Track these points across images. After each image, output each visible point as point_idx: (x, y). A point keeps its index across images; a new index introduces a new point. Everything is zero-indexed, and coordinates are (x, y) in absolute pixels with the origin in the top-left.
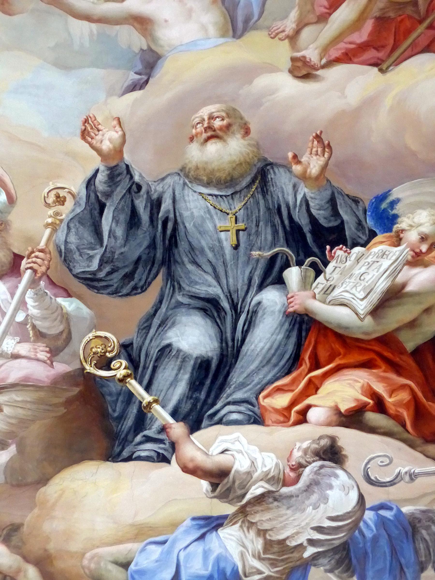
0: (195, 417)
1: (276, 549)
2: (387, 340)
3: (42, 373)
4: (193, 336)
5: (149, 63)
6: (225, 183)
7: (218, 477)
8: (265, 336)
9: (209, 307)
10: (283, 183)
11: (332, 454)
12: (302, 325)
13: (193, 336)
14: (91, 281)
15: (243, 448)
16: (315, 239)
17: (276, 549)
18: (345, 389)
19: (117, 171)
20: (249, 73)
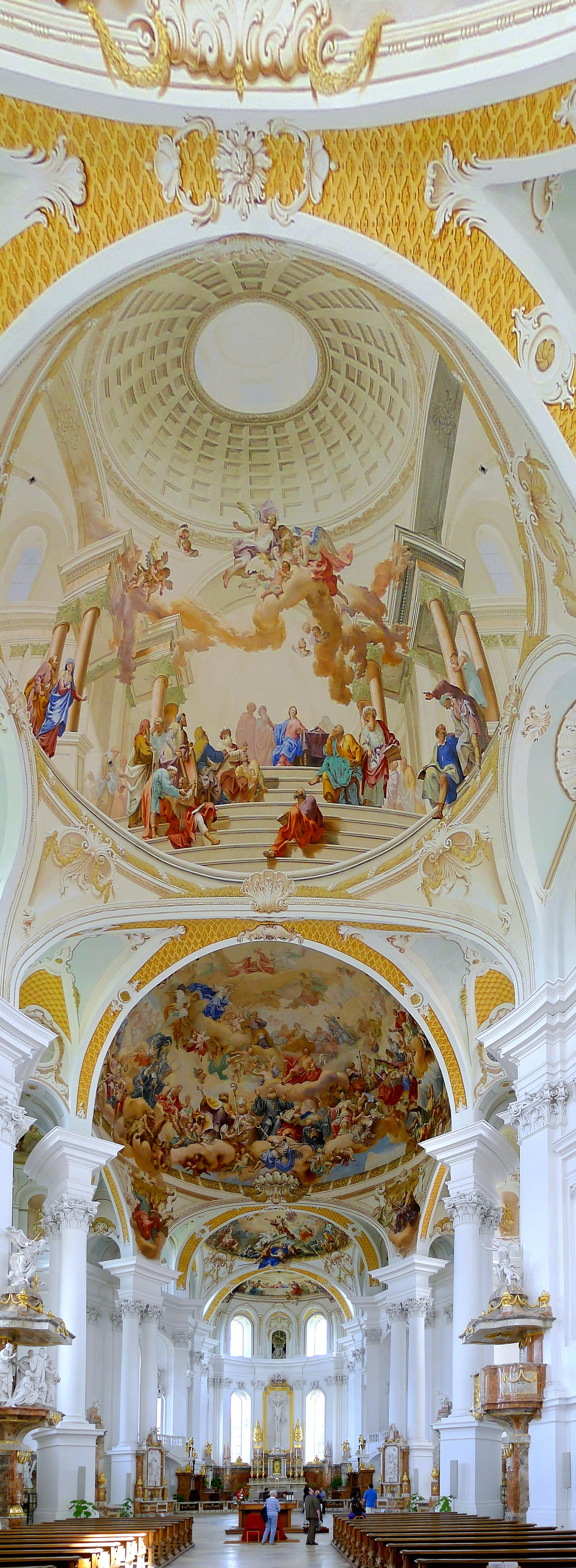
0: (269, 1134)
1: (279, 1154)
2: (292, 1124)
3: (251, 1128)
4: (269, 1122)
5: (263, 1081)
7: (272, 1143)
8: (277, 1122)
9: (271, 1118)
10: (280, 1100)
11: (285, 1140)
12: (282, 1121)
13: (269, 1122)
14: (256, 1114)
15: (275, 1139)
16: (284, 1108)
17: (279, 1154)
18: (287, 1131)
19: (259, 1098)
20: (276, 1084)
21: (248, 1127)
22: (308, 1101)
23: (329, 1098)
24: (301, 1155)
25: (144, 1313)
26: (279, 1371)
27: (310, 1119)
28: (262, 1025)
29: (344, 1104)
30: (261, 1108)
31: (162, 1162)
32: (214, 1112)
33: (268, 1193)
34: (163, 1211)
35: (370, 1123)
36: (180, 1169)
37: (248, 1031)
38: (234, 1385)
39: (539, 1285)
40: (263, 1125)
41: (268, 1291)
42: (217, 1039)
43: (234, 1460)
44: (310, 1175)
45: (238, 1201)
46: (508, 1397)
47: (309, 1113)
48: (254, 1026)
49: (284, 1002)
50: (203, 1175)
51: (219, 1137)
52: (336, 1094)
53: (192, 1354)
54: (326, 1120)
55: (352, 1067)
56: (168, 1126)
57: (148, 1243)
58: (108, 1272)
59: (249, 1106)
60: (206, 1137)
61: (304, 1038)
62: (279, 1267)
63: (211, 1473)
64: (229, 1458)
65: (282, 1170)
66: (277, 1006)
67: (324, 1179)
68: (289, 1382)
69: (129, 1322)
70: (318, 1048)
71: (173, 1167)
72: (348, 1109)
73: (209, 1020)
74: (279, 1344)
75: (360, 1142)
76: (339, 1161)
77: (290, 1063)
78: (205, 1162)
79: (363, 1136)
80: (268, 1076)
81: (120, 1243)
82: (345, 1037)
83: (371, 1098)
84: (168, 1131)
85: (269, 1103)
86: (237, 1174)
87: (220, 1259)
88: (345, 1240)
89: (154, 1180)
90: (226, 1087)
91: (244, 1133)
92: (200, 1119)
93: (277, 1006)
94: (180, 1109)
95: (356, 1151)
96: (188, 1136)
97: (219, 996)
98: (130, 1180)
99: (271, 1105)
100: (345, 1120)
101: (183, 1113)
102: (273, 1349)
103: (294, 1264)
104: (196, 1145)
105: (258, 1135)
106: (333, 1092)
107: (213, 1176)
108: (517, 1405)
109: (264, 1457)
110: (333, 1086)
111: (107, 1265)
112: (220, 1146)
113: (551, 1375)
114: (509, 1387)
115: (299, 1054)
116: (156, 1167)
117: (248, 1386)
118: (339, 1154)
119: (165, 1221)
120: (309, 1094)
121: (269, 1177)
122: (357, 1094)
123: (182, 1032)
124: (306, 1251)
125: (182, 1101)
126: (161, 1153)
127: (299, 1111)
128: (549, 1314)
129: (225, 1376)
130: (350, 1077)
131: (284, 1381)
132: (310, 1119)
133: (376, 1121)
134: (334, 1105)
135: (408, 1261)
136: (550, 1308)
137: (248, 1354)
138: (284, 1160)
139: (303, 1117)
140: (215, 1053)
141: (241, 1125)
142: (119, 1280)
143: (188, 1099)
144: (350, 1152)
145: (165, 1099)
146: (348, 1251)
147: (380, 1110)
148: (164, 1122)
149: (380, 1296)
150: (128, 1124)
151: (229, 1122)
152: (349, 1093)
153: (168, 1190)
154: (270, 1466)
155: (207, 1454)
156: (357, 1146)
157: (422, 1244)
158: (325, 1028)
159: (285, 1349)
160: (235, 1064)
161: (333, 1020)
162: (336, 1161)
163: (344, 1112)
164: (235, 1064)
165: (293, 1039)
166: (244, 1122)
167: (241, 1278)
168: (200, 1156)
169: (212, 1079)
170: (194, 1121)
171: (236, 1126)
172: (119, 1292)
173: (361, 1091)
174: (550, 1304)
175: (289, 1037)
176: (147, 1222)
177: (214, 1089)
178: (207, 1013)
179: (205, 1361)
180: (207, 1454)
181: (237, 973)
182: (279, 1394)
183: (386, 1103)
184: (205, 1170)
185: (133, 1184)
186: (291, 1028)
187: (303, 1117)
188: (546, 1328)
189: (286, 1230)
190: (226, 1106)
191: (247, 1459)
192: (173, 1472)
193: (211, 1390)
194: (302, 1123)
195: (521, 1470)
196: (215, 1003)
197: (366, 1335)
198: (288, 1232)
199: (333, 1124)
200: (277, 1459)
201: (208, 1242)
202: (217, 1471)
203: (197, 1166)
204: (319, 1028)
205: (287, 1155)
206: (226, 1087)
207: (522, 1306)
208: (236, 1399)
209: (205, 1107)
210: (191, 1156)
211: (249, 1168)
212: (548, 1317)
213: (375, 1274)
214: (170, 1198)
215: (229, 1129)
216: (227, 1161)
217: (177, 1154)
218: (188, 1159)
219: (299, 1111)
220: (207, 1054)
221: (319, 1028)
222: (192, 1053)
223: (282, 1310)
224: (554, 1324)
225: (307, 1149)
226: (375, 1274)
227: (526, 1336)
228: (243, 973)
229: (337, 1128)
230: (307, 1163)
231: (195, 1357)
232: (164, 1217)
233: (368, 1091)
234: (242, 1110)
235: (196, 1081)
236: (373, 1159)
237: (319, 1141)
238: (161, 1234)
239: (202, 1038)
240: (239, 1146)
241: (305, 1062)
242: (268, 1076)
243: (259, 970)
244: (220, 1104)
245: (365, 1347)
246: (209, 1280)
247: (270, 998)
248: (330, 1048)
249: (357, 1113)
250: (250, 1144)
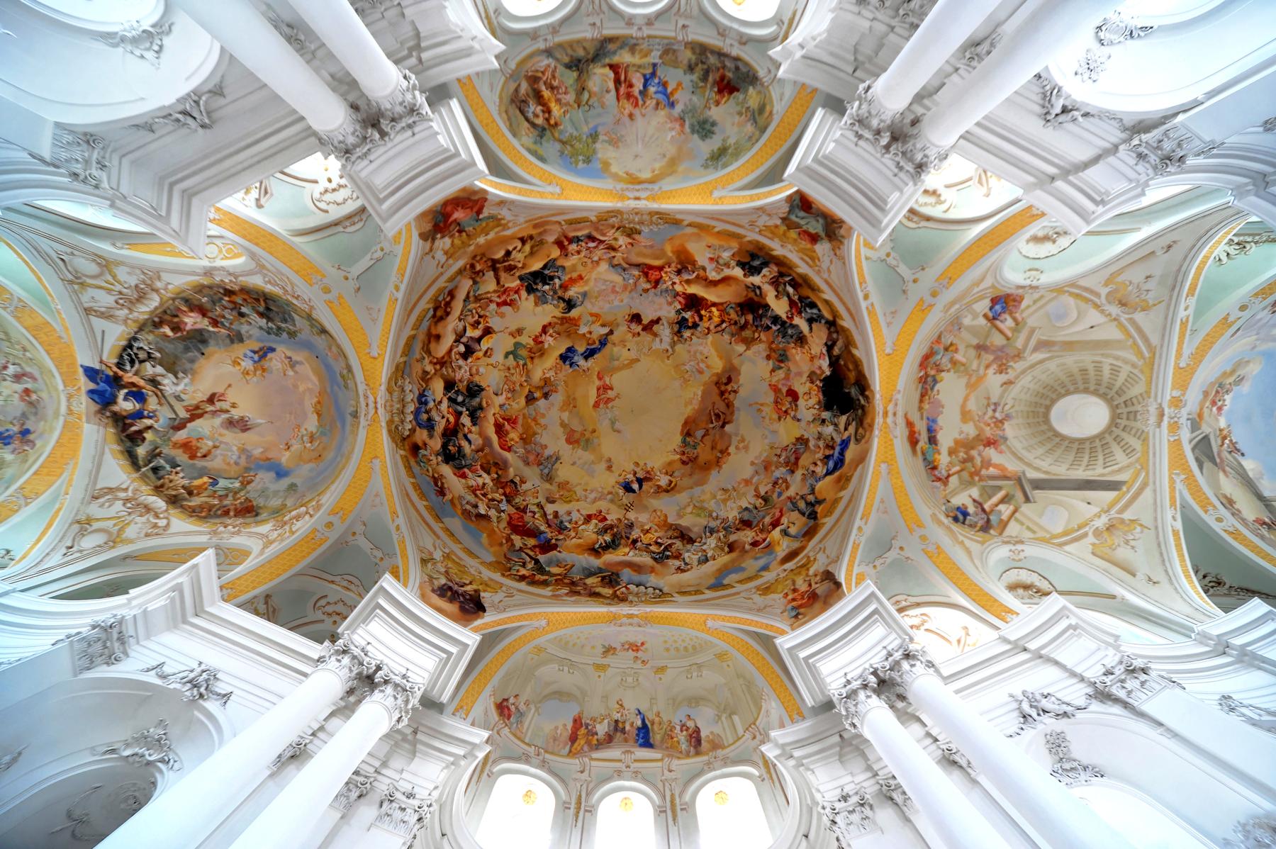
0: (450, 399)
4: (460, 399)
6: (480, 404)
8: (460, 408)
12: (461, 413)
13: (460, 399)
18: (452, 419)
21: (458, 377)
22: (480, 441)
23: (488, 463)
24: (431, 436)
27: (464, 443)
28: (546, 396)
29: (486, 479)
30: (474, 390)
32: (479, 340)
33: (396, 394)
35: (483, 512)
36: (450, 286)
37: (542, 383)
40: (457, 392)
42: (542, 355)
44: (415, 449)
45: (395, 352)
47: (470, 442)
48: (547, 389)
49: (565, 416)
50: (431, 312)
51: (456, 341)
52: (493, 469)
54: (468, 462)
55: (523, 482)
59: (476, 379)
61: (535, 434)
65: (417, 413)
66: (562, 409)
67: (416, 469)
70: (528, 447)
73: (563, 350)
76: (436, 485)
77: (512, 421)
78: (441, 319)
79: (468, 507)
80: (501, 399)
82: (546, 471)
83: (504, 506)
84: (489, 285)
85: (478, 400)
86: (418, 356)
90: (498, 357)
91: (454, 371)
92: (478, 323)
93: (562, 409)
94: (498, 305)
95: (452, 501)
97: (582, 362)
99: (475, 402)
100: (474, 483)
101: (493, 306)
104: (458, 313)
105: (449, 385)
106: (495, 466)
107: (426, 324)
110: (501, 465)
112: (449, 340)
115: (520, 429)
120: (487, 442)
121: (409, 397)
122: (501, 491)
123: (566, 325)
125: (505, 309)
130: (512, 481)
132: (464, 443)
133: (486, 517)
134: (483, 468)
138: (425, 416)
140: (530, 351)
141: (460, 367)
143: (502, 315)
144: (449, 497)
145: (516, 292)
147: (499, 520)
148: (498, 283)
151: (465, 356)
152: (498, 482)
156: (456, 502)
158: (547, 453)
160: (515, 368)
161: (558, 459)
162: (435, 480)
163: (480, 481)
164: (515, 368)
165: (533, 424)
166: (462, 371)
168: (448, 314)
169: (509, 343)
170: (480, 317)
171: (461, 362)
173: (504, 494)
175: (535, 419)
177: (499, 344)
178: (570, 350)
181: (600, 378)
183: (509, 523)
184: (434, 316)
186: (542, 421)
187: (465, 436)
190: (480, 354)
194: (460, 435)
196: (576, 358)
204: (546, 447)
205: (430, 419)
206: (498, 357)
210: (453, 304)
211: (420, 372)
214: (443, 259)
220: (532, 343)
221: (546, 447)
222: (540, 329)
225: (436, 443)
228: (597, 383)
229: (464, 476)
230: (425, 445)
233: (509, 501)
234: (474, 370)
235: (513, 328)
236: (456, 523)
237: (448, 457)
239: (548, 340)
240: (442, 363)
241: (514, 435)
242: (501, 399)
243: (599, 396)
247: (571, 404)
248: (532, 458)
249: (485, 495)
250: (442, 376)
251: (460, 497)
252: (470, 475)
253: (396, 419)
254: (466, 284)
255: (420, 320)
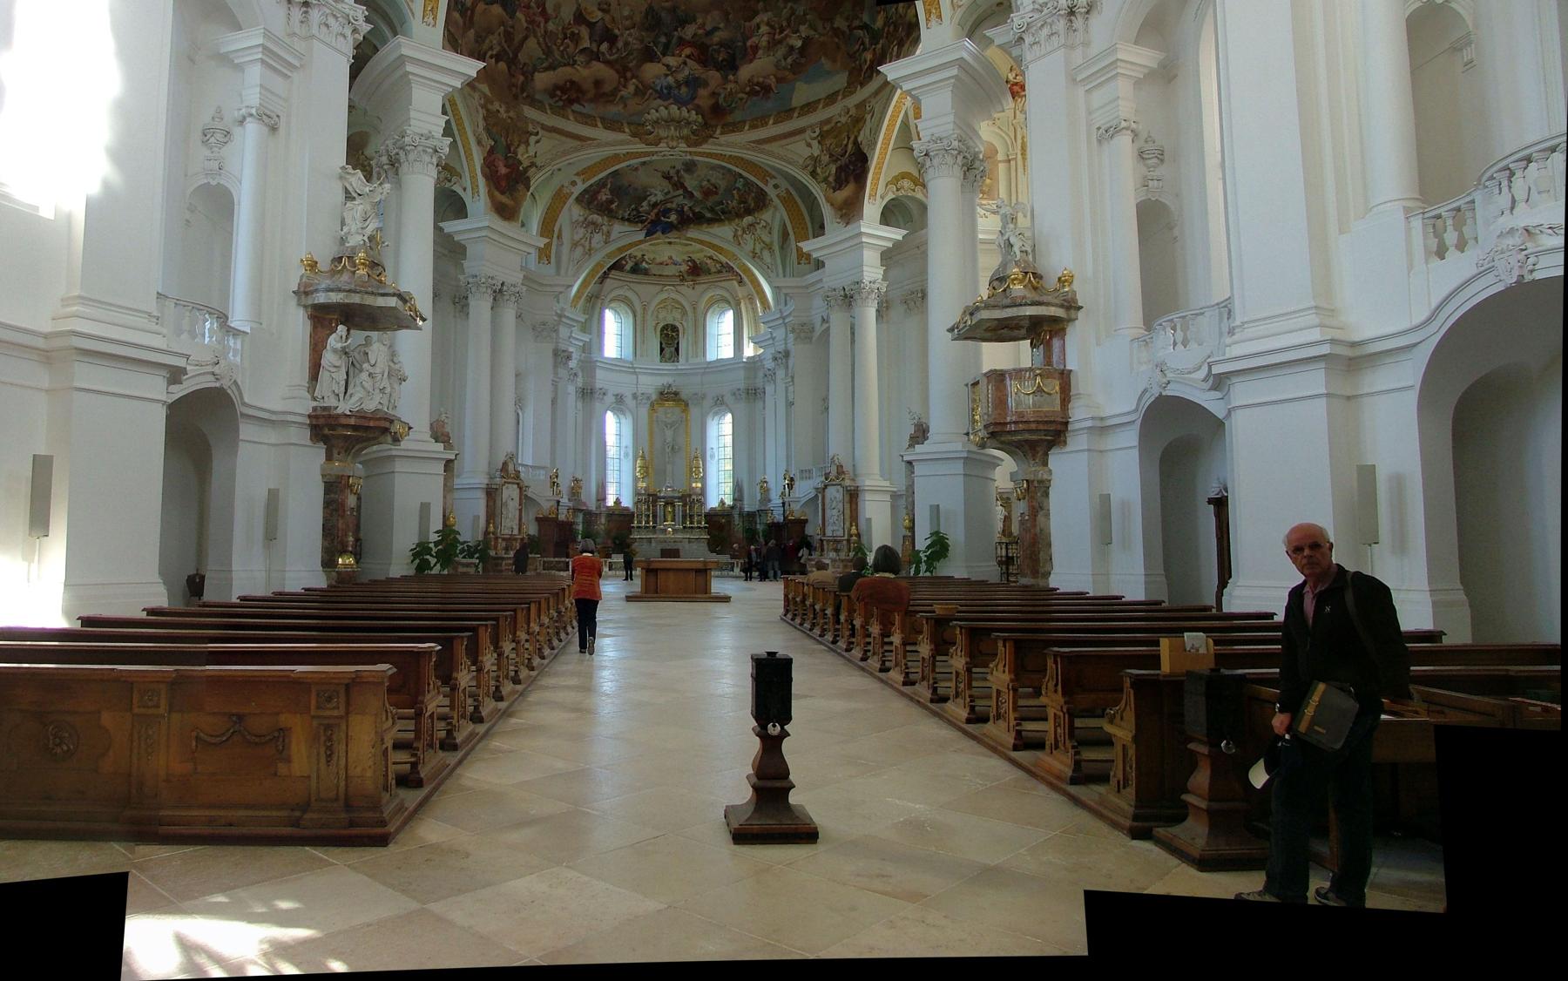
1: (677, 81)
4: (663, 39)
8: (674, 41)
12: (680, 38)
13: (663, 39)
15: (672, 61)
16: (683, 22)
18: (688, 51)
22: (716, 13)
24: (705, 84)
25: (498, 293)
26: (670, 380)
29: (763, 17)
30: (652, 21)
31: (523, 90)
32: (591, 25)
34: (524, 155)
35: (799, 43)
36: (547, 100)
38: (610, 399)
39: (1058, 260)
41: (654, 269)
43: (610, 502)
45: (622, 143)
46: (1021, 414)
47: (716, 29)
50: (576, 107)
53: (556, 353)
56: (532, 43)
57: (504, 199)
58: (450, 236)
59: (638, 18)
60: (580, 59)
62: (673, 236)
63: (580, 518)
64: (604, 499)
67: (737, 116)
68: (683, 396)
69: (480, 306)
71: (537, 97)
72: (768, 24)
74: (670, 341)
75: (785, 68)
76: (757, 93)
79: (789, 60)
81: (467, 197)
84: (532, 48)
85: (663, 15)
86: (621, 107)
87: (593, 223)
88: (761, 201)
89: (512, 114)
91: (630, 53)
95: (779, 80)
96: (557, 55)
98: (482, 112)
100: (765, 38)
101: (551, 26)
102: (662, 350)
103: (693, 233)
104: (568, 69)
105: (649, 56)
107: (588, 109)
108: (1033, 426)
109: (649, 499)
111: (451, 226)
112: (599, 69)
113: (1079, 385)
114: (1022, 399)
116: (516, 97)
117: (629, 401)
118: (758, 84)
119: (526, 170)
121: (664, 112)
124: (709, 215)
126: (522, 78)
127: (702, 26)
128: (1075, 301)
129: (598, 385)
131: (676, 394)
133: (807, 41)
134: (750, 19)
135: (850, 230)
136: (1074, 293)
137: (628, 354)
138: (684, 90)
139: (709, 34)
141: (626, 44)
142: (464, 248)
144: (772, 81)
146: (766, 216)
147: (812, 27)
149: (813, 277)
150: (480, 39)
151: (612, 39)
153: (530, 128)
154: (660, 512)
155: (574, 493)
157: (872, 209)
159: (677, 350)
162: (753, 93)
163: (764, 29)
166: (631, 38)
167: (621, 250)
168: (572, 82)
171: (620, 44)
172: (466, 264)
174: (1075, 286)
176: (503, 170)
179: (573, 364)
180: (574, 493)
182: (670, 412)
184: (577, 100)
185: (485, 119)
187: (709, 34)
188: (1071, 320)
189: (683, 186)
190: (607, 18)
191: (627, 502)
192: (532, 516)
193: (580, 405)
195: (1040, 518)
197: (793, 331)
198: (685, 189)
199: (749, 43)
200: (669, 502)
201: (579, 200)
202: (590, 517)
203: (568, 96)
205: (687, 83)
207: (1035, 289)
208: (610, 418)
209: (580, 17)
212: (1071, 305)
213: (806, 246)
214: (533, 139)
215: (610, 49)
216: (607, 88)
217: (543, 79)
218: (557, 87)
219: (702, 26)
223: (674, 295)
224: (1081, 314)
225: (714, 76)
226: (806, 246)
227: (1042, 332)
229: (756, 48)
230: (714, 94)
231: (561, 356)
232: (526, 164)
234: (628, 23)
236: (803, 92)
237: (731, 65)
238: (521, 187)
240: (623, 71)
244: (600, 14)
245: (791, 346)
246: (579, 251)
250: (638, 67)
251: (777, 66)
252: (755, 39)
253: (686, 132)
254: (543, 79)
255: (587, 120)
